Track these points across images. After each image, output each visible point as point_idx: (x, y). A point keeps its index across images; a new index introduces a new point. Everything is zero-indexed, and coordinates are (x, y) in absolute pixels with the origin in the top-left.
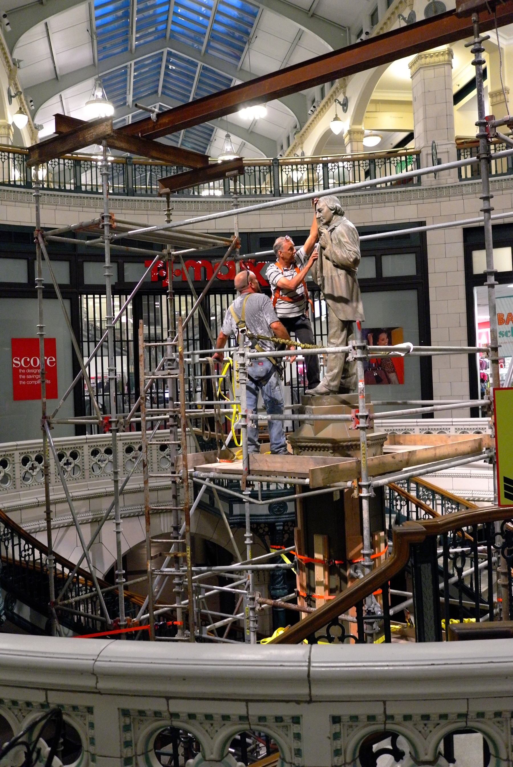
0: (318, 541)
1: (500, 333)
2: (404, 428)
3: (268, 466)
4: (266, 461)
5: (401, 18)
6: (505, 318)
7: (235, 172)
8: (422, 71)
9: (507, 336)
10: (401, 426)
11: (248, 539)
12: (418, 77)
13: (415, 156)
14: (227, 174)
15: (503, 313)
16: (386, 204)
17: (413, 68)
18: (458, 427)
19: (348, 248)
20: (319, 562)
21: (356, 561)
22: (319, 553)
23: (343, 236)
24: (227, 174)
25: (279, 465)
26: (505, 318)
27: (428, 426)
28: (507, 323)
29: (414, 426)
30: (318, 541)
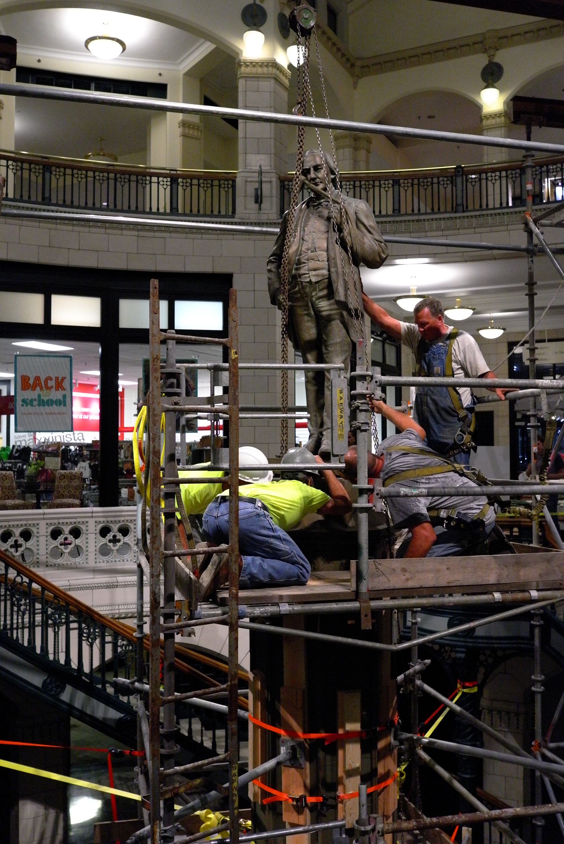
0: (351, 702)
1: (23, 401)
2: (25, 522)
6: (31, 382)
9: (32, 405)
10: (21, 520)
15: (30, 375)
18: (49, 521)
20: (350, 736)
25: (430, 575)
26: (31, 382)
27: (58, 518)
28: (34, 389)
29: (38, 519)
30: (351, 702)
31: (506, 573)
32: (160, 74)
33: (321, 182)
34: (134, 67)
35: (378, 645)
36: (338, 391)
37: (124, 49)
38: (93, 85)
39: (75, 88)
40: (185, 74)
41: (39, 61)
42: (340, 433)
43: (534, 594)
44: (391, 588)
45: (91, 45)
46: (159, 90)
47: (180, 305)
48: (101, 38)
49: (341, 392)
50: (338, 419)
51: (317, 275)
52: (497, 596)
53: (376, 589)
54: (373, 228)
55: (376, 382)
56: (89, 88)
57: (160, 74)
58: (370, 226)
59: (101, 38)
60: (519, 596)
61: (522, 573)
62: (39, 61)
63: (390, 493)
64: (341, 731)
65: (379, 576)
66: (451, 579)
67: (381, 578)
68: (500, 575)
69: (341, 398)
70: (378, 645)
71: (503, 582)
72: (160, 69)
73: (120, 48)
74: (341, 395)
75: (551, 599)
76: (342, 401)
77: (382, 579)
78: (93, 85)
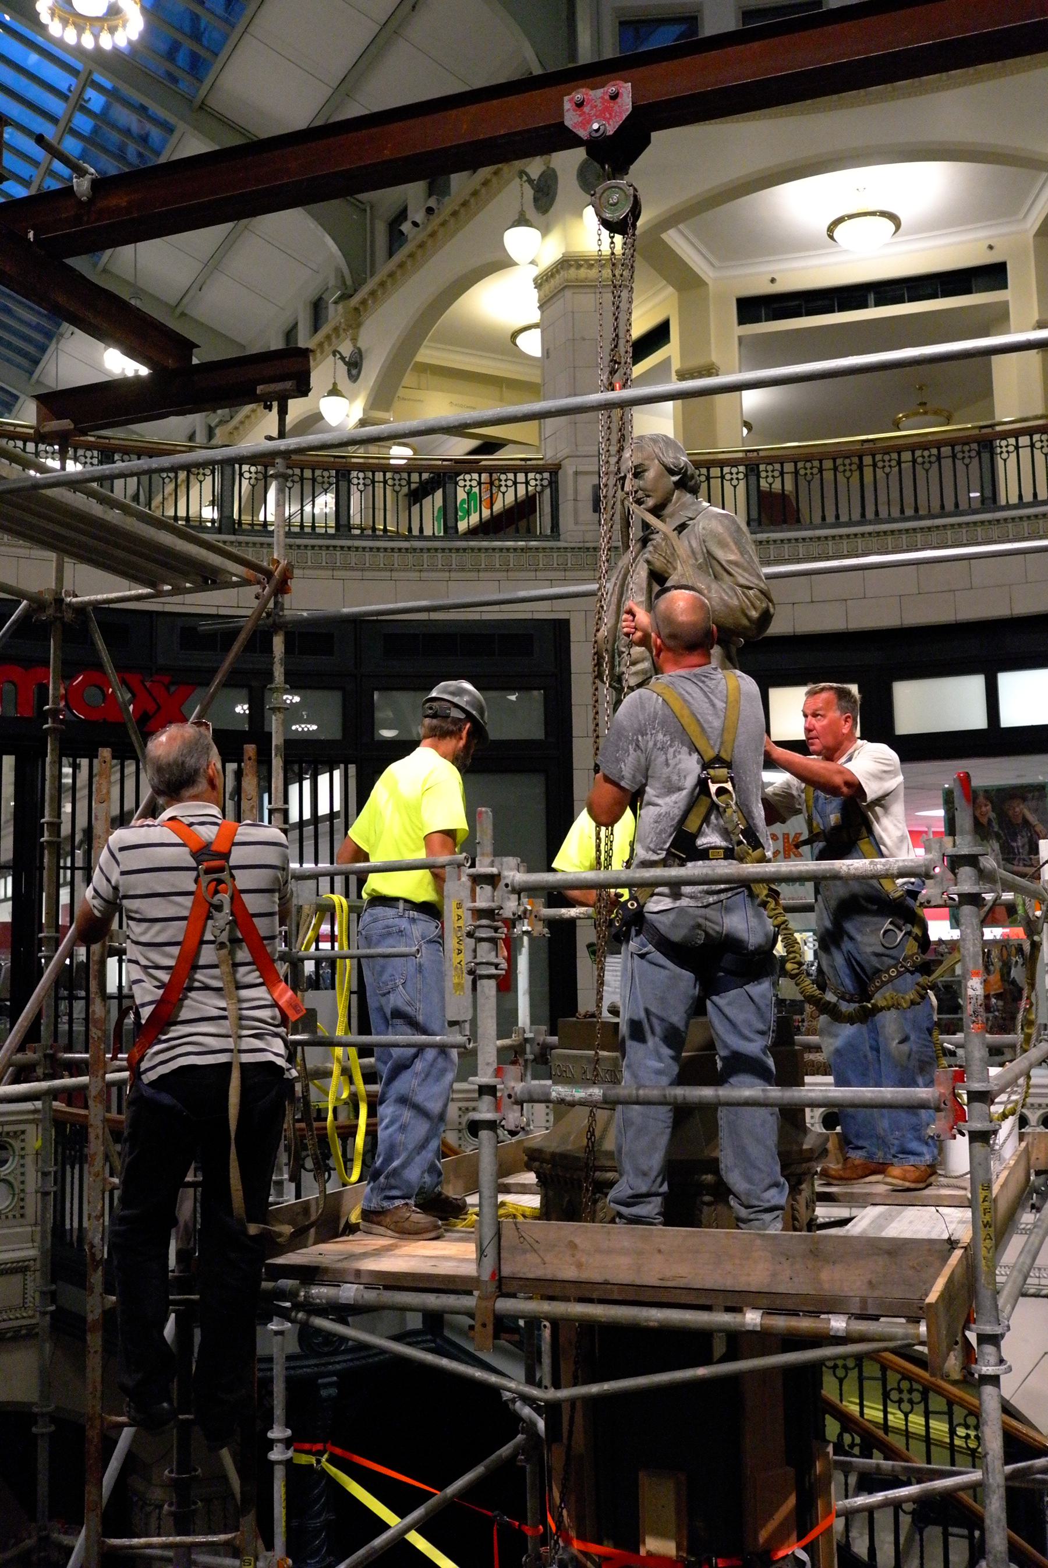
0: (659, 1496)
3: (579, 1266)
4: (573, 1246)
5: (525, 178)
7: (288, 385)
8: (568, 293)
11: (278, 1448)
12: (558, 306)
13: (546, 475)
14: (260, 389)
16: (481, 574)
17: (546, 287)
19: (742, 581)
21: (781, 1554)
22: (661, 1534)
23: (723, 545)
24: (260, 389)
25: (624, 1261)
30: (659, 1496)
31: (788, 1273)
32: (991, 247)
33: (648, 496)
34: (959, 243)
35: (594, 1389)
36: (454, 905)
37: (898, 224)
38: (871, 298)
39: (841, 310)
40: (1035, 236)
41: (773, 280)
42: (456, 981)
43: (838, 1324)
44: (549, 1277)
45: (836, 234)
46: (992, 275)
47: (1007, 681)
48: (851, 217)
49: (459, 906)
50: (454, 955)
51: (636, 673)
52: (752, 1318)
53: (521, 1275)
54: (736, 564)
55: (507, 885)
56: (864, 305)
57: (991, 247)
58: (730, 562)
59: (851, 217)
60: (805, 1324)
61: (825, 1275)
62: (773, 280)
63: (530, 1093)
64: (643, 1552)
65: (525, 1252)
66: (668, 1274)
67: (528, 1255)
68: (774, 1275)
69: (459, 918)
70: (594, 1389)
71: (781, 1289)
72: (990, 237)
73: (890, 226)
74: (460, 912)
75: (891, 1340)
76: (461, 923)
77: (531, 1258)
78: (871, 298)
